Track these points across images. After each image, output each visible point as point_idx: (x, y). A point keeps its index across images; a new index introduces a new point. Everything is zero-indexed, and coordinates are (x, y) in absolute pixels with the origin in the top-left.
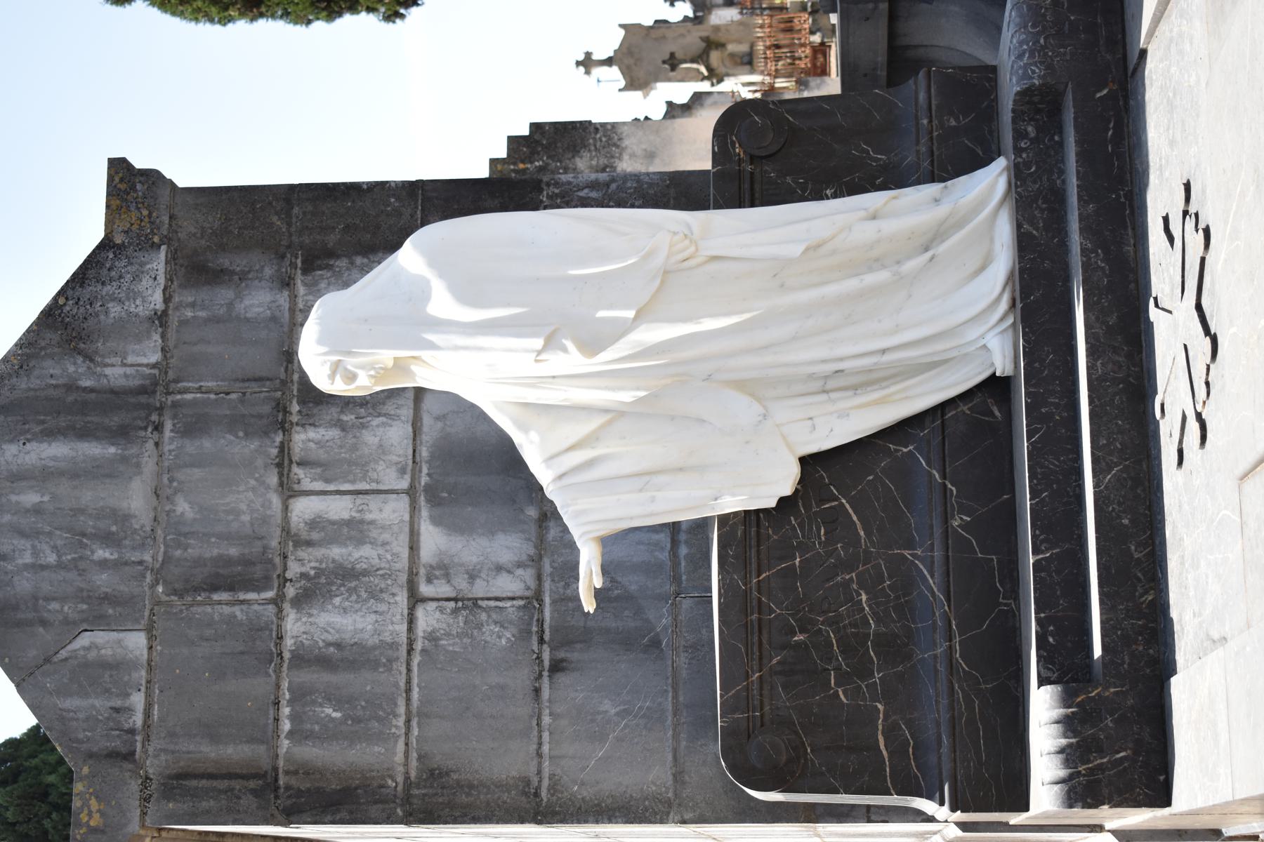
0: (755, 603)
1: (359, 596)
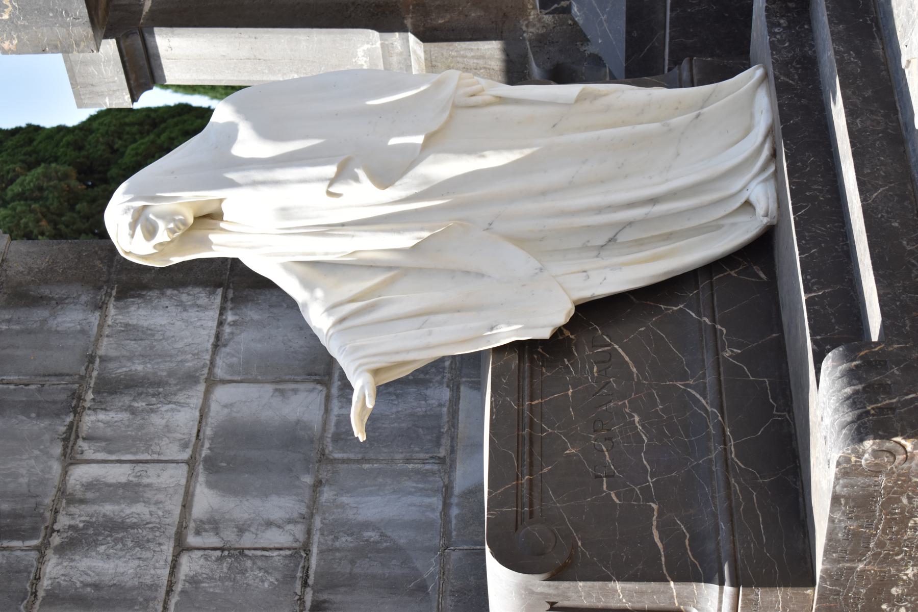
0: (527, 420)
1: (124, 545)
